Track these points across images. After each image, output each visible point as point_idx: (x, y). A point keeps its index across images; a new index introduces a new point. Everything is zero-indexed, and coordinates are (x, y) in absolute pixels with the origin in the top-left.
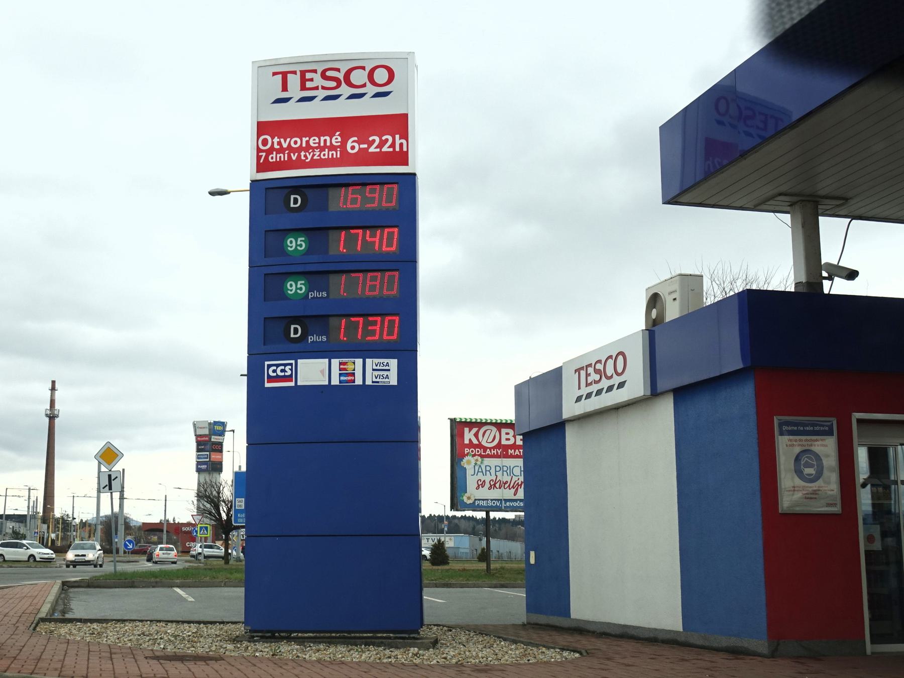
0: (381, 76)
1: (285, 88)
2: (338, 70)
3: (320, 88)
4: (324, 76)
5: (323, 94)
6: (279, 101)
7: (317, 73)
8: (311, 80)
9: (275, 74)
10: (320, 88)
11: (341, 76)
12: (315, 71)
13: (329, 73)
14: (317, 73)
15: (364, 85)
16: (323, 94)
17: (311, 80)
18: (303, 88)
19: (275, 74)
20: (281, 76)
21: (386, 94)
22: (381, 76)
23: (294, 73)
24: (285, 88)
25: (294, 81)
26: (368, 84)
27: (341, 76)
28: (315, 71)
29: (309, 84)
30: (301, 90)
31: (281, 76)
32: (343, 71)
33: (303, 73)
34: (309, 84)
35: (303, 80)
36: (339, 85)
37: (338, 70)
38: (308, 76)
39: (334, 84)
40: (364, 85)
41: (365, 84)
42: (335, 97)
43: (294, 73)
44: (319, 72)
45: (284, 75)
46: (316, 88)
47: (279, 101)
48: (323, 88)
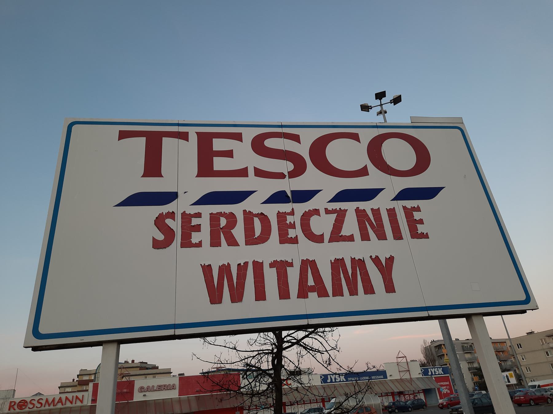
3: (251, 172)
7: (241, 140)
8: (229, 154)
10: (251, 172)
12: (238, 137)
14: (241, 140)
15: (363, 172)
17: (229, 154)
20: (144, 139)
26: (371, 168)
30: (199, 175)
31: (144, 139)
37: (296, 138)
39: (286, 166)
40: (363, 172)
41: (365, 168)
43: (184, 136)
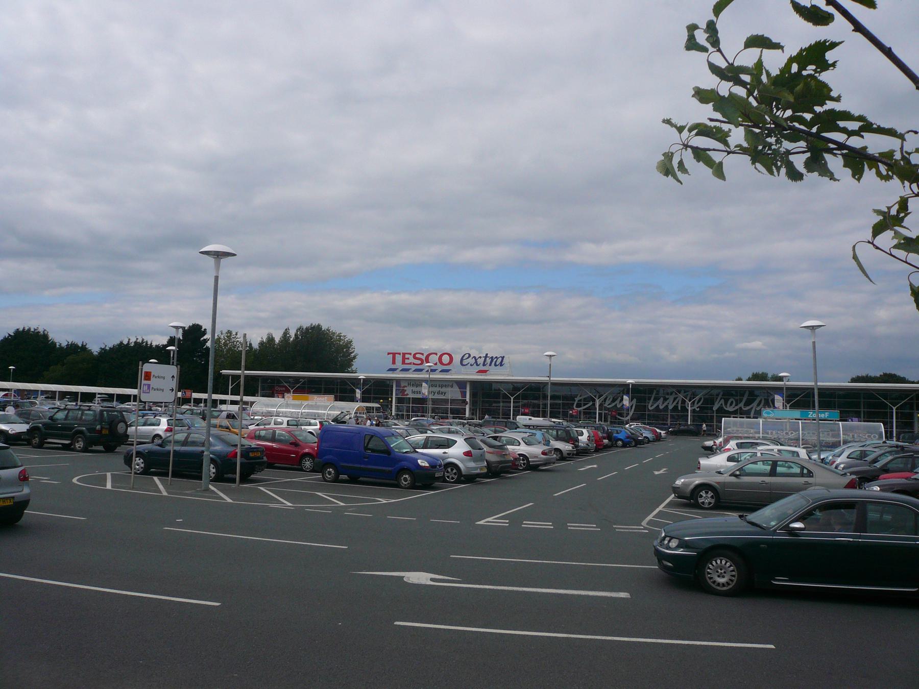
0: (446, 359)
1: (394, 362)
2: (423, 354)
4: (415, 357)
5: (414, 367)
6: (391, 370)
8: (408, 359)
9: (389, 354)
11: (424, 358)
12: (410, 354)
13: (417, 356)
16: (414, 367)
17: (408, 359)
18: (403, 363)
19: (389, 354)
21: (447, 371)
22: (446, 359)
23: (399, 354)
24: (394, 362)
25: (399, 358)
26: (438, 363)
27: (424, 358)
28: (410, 354)
29: (407, 361)
32: (425, 355)
33: (404, 354)
34: (407, 361)
35: (404, 359)
36: (422, 363)
37: (423, 354)
38: (407, 356)
39: (419, 362)
42: (421, 370)
43: (399, 354)
44: (412, 355)
45: (394, 354)
46: (410, 364)
47: (391, 370)
48: (414, 364)
